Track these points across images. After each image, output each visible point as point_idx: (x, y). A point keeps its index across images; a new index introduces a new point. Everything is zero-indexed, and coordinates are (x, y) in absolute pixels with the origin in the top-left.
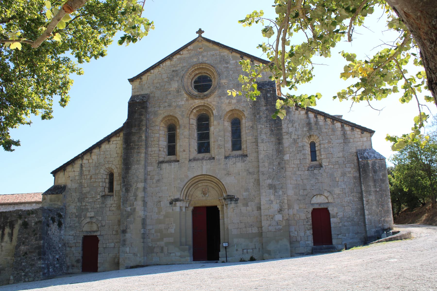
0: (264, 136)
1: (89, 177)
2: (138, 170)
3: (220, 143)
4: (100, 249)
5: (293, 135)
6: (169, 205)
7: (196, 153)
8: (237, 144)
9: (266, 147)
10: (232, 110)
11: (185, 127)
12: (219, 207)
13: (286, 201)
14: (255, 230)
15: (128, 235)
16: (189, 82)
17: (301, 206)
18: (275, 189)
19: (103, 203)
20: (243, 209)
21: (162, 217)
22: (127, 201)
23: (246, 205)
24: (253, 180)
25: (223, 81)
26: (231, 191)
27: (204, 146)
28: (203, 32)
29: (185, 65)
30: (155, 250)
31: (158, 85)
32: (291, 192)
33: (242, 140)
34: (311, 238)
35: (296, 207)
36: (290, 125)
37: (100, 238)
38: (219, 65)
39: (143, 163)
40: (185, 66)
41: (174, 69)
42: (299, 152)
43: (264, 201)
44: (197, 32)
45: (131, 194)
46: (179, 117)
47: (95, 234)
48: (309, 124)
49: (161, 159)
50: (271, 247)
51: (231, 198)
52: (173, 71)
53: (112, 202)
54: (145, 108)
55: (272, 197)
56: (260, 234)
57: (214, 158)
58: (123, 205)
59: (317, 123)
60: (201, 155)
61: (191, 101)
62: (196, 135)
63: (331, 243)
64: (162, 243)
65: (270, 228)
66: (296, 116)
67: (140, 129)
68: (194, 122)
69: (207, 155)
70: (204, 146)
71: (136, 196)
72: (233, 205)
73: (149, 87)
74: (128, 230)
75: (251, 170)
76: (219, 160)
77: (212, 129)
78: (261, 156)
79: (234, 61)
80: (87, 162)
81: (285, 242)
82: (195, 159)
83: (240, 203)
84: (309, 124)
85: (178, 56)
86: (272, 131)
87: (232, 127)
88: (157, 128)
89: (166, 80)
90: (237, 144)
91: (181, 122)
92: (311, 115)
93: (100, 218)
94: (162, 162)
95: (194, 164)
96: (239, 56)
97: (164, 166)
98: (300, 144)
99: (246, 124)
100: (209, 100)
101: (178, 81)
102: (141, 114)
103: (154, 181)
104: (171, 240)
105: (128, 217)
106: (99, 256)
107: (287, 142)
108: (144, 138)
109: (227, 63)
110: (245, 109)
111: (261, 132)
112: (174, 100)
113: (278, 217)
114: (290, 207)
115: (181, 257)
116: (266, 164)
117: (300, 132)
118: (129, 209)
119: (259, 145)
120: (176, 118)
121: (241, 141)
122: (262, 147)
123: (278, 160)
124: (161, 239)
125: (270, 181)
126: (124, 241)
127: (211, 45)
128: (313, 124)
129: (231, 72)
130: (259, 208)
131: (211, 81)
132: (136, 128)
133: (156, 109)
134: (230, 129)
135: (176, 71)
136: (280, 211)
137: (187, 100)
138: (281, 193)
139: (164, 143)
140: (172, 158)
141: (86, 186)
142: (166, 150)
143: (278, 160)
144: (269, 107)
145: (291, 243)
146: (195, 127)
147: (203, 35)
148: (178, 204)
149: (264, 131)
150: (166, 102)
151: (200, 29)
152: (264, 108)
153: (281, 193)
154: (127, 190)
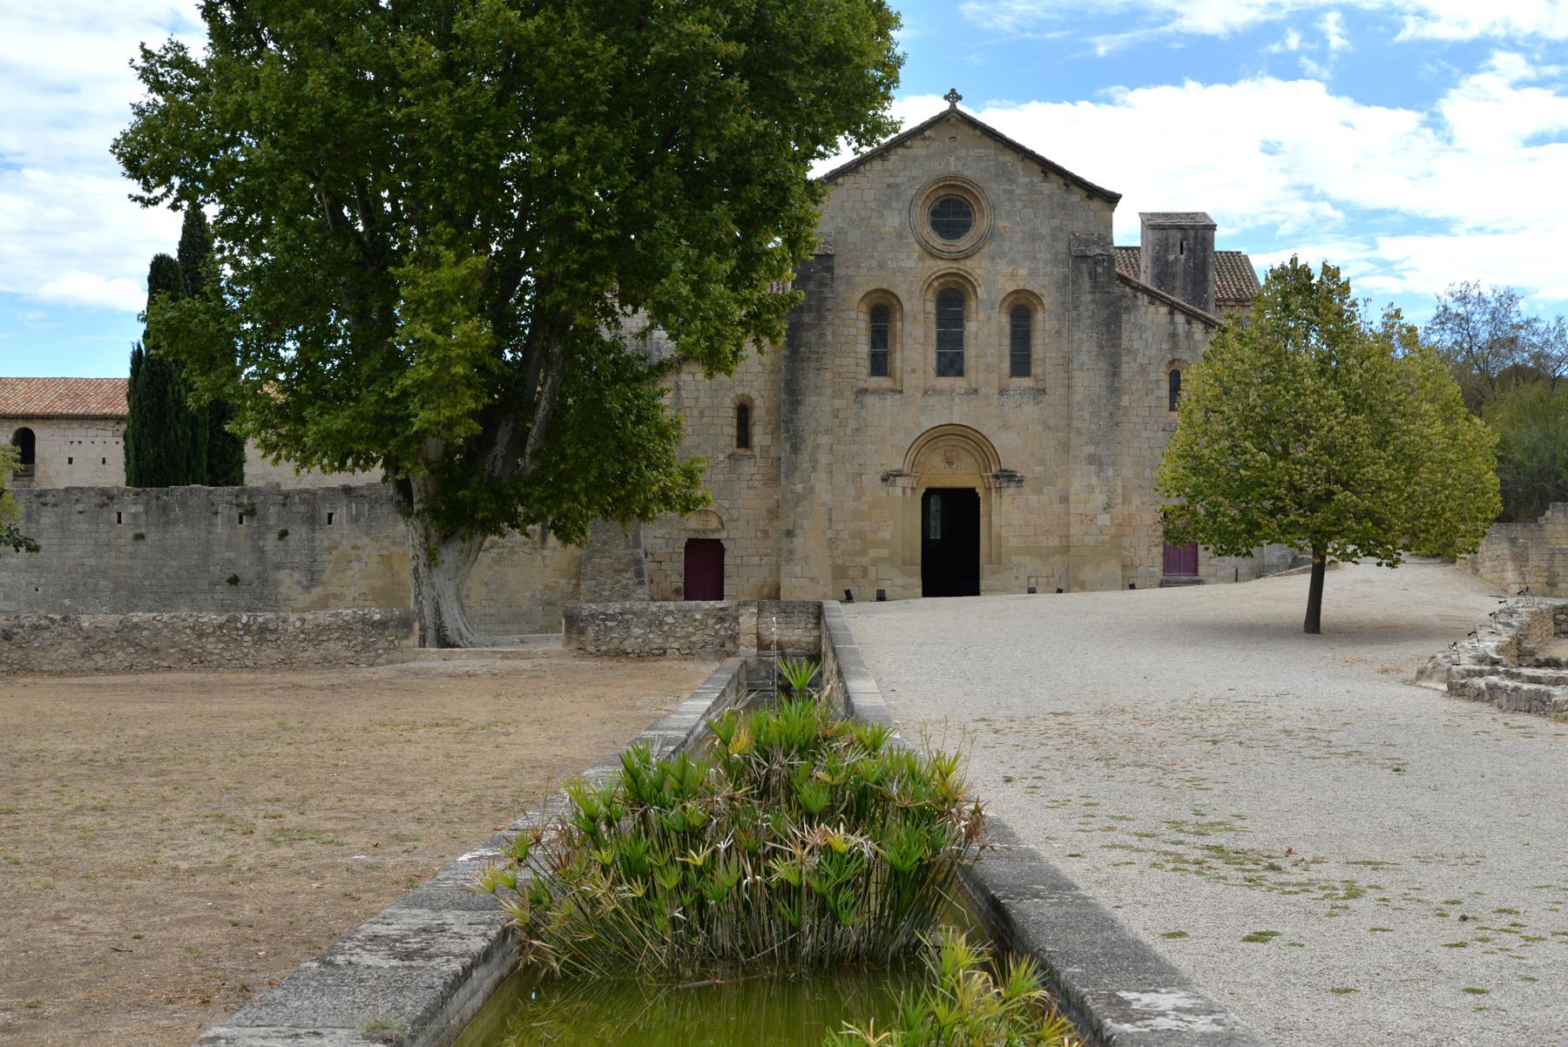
0: (1084, 358)
1: (696, 413)
2: (820, 406)
3: (989, 360)
4: (729, 568)
5: (1140, 356)
6: (879, 482)
7: (932, 372)
8: (1021, 363)
9: (1088, 380)
10: (1016, 292)
11: (915, 318)
12: (980, 492)
13: (1119, 490)
14: (1054, 541)
15: (798, 542)
16: (922, 218)
17: (1146, 499)
18: (1101, 464)
19: (732, 470)
20: (1033, 499)
21: (865, 507)
22: (795, 470)
23: (1039, 491)
24: (1055, 443)
25: (1002, 223)
26: (1008, 463)
27: (951, 363)
28: (960, 98)
29: (916, 173)
30: (850, 573)
31: (854, 216)
32: (1128, 472)
33: (1034, 357)
34: (1160, 560)
35: (1136, 501)
36: (1135, 336)
37: (726, 544)
38: (994, 185)
39: (829, 391)
40: (915, 178)
41: (892, 180)
42: (1149, 392)
43: (1077, 486)
44: (946, 98)
45: (804, 459)
46: (903, 296)
47: (716, 536)
48: (1173, 336)
49: (862, 385)
50: (1087, 574)
51: (1009, 477)
52: (889, 185)
53: (753, 470)
54: (830, 269)
55: (1094, 481)
56: (1066, 549)
57: (976, 391)
58: (787, 477)
59: (1189, 335)
60: (946, 382)
61: (930, 262)
62: (934, 336)
63: (1196, 572)
64: (864, 560)
65: (1087, 539)
66: (1150, 317)
67: (821, 318)
68: (931, 307)
69: (958, 383)
70: (951, 363)
71: (814, 462)
72: (1010, 491)
73: (832, 218)
74: (799, 532)
75: (1051, 422)
76: (987, 396)
77: (971, 327)
78: (1077, 398)
79: (1027, 180)
80: (690, 378)
81: (1114, 567)
82: (936, 392)
83: (1026, 489)
84: (1173, 336)
85: (901, 151)
86: (1101, 347)
87: (1013, 326)
88: (853, 315)
89: (873, 205)
90: (1021, 363)
91: (907, 306)
92: (1180, 318)
93: (726, 504)
94: (865, 391)
95: (932, 401)
96: (1037, 168)
97: (870, 400)
98: (1153, 377)
99: (1044, 324)
100: (969, 263)
101: (900, 211)
102: (822, 284)
103: (849, 431)
104: (885, 553)
105: (797, 504)
106: (726, 581)
107: (1127, 371)
108: (829, 337)
109: (1011, 181)
110: (1044, 292)
111: (1079, 347)
112: (890, 255)
113: (1104, 519)
114: (1126, 500)
115: (903, 587)
116: (1086, 415)
117: (1154, 352)
118: (799, 488)
119: (1075, 374)
120: (894, 295)
121: (1029, 356)
122: (1080, 378)
123: (1110, 408)
124: (863, 552)
125: (1091, 449)
126: (791, 552)
127: (978, 133)
128: (1182, 338)
129: (1019, 205)
130: (1065, 499)
131: (969, 214)
132: (812, 315)
133: (851, 271)
134: (1008, 328)
135: (897, 186)
136: (1107, 507)
137: (920, 258)
138: (1110, 472)
139: (864, 348)
140: (885, 382)
141: (690, 430)
142: (867, 363)
143: (1110, 408)
144: (1097, 296)
145: (1124, 567)
146: (933, 318)
147: (960, 106)
148: (900, 481)
149: (1086, 346)
150: (872, 257)
151: (953, 91)
152: (1089, 297)
153: (1110, 472)
154: (795, 449)
